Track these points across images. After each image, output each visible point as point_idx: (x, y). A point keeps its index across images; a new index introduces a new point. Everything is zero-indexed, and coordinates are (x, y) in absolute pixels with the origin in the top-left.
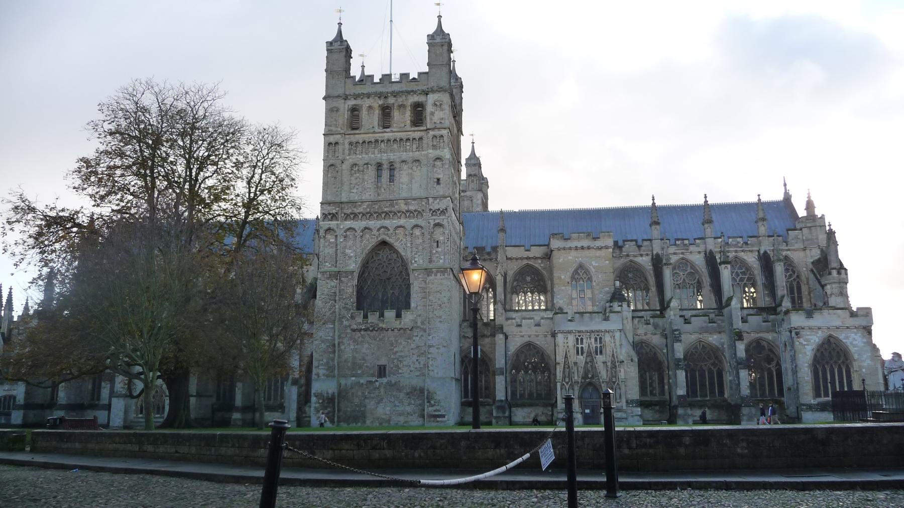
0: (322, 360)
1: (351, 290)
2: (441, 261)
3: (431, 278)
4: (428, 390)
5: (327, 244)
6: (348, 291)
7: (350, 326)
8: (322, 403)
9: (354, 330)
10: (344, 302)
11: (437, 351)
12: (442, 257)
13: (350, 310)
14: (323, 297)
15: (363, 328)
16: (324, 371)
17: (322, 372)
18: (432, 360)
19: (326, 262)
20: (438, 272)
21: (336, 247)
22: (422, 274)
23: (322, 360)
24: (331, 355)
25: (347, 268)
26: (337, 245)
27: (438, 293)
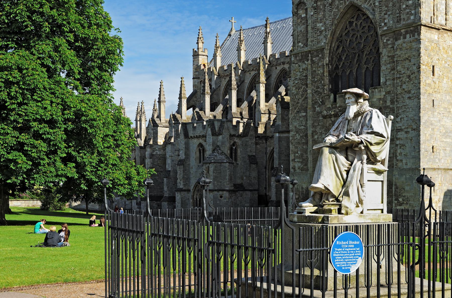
0: (297, 153)
1: (322, 71)
2: (412, 17)
3: (400, 42)
4: (396, 185)
5: (299, 20)
6: (319, 72)
7: (321, 112)
8: (298, 198)
9: (325, 117)
10: (316, 85)
11: (405, 135)
12: (413, 12)
13: (321, 93)
14: (296, 82)
15: (333, 113)
16: (300, 164)
17: (297, 165)
18: (400, 148)
19: (299, 42)
20: (407, 32)
21: (307, 23)
22: (391, 39)
23: (297, 153)
24: (304, 147)
25: (319, 45)
26: (307, 21)
27: (407, 61)
